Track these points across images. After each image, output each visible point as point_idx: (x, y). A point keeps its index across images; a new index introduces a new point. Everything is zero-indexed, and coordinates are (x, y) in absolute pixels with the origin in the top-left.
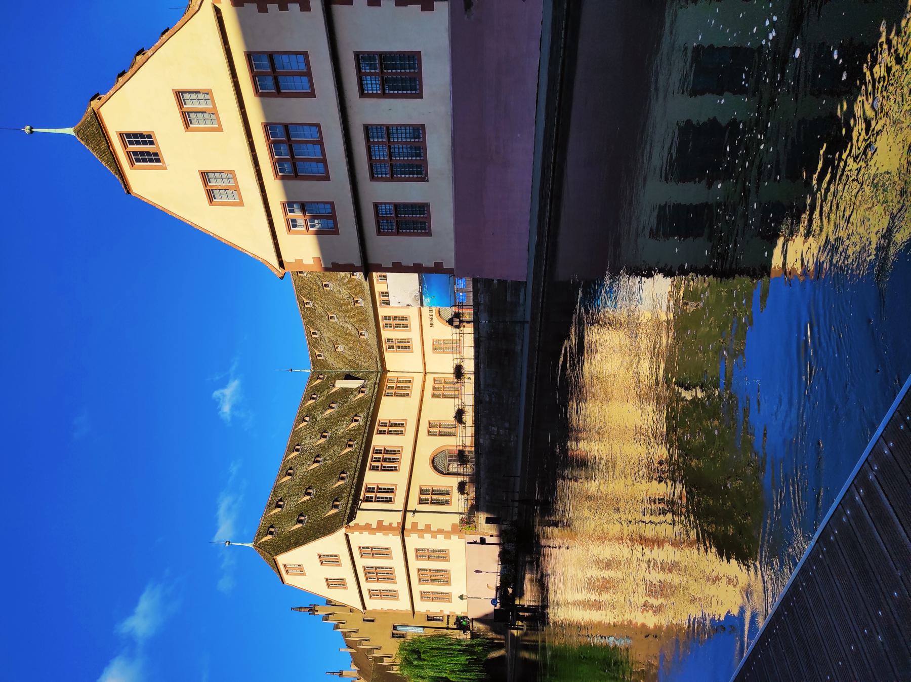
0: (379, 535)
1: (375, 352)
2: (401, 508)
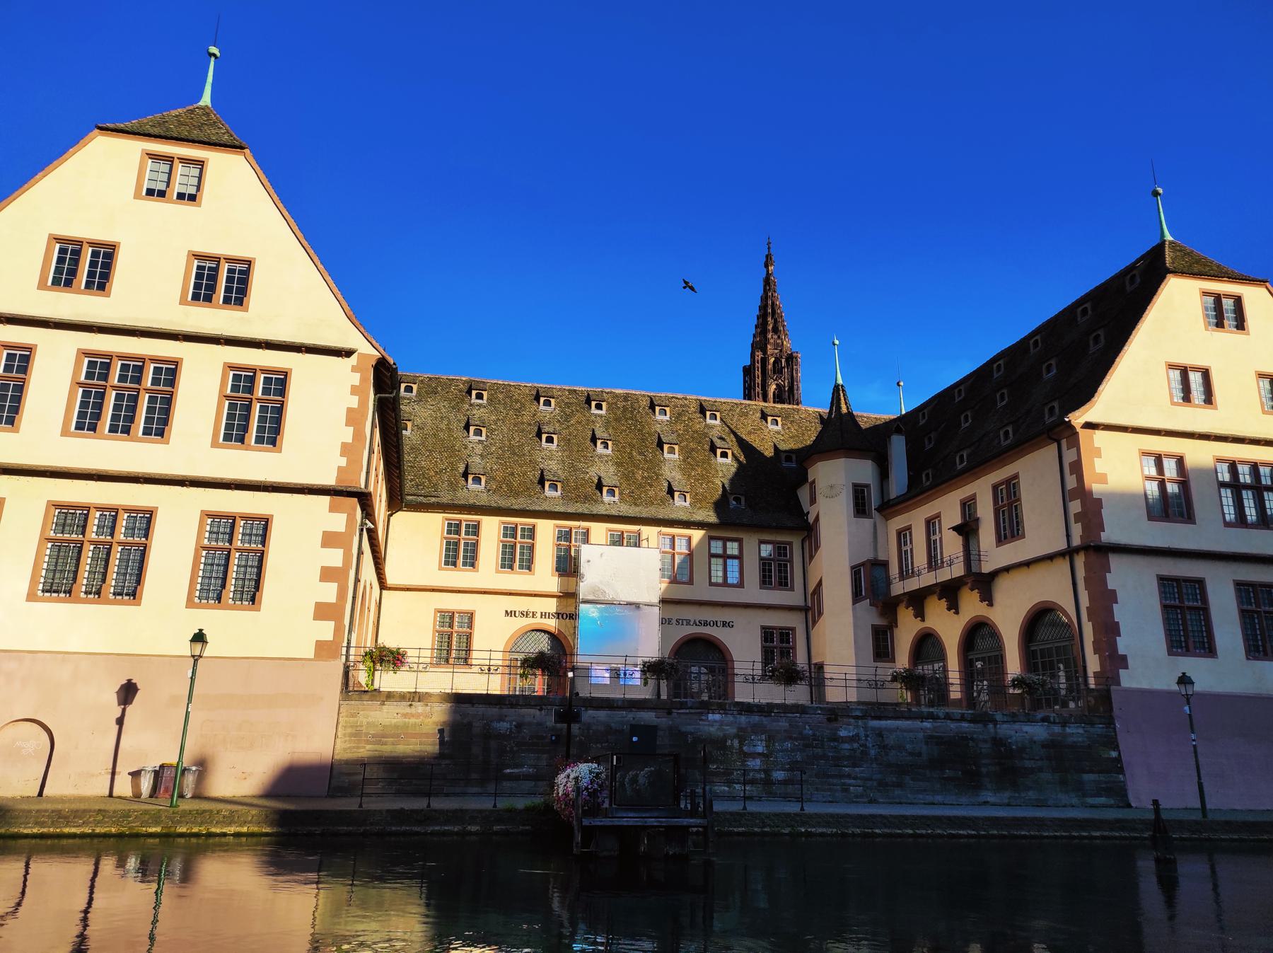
1: (445, 498)
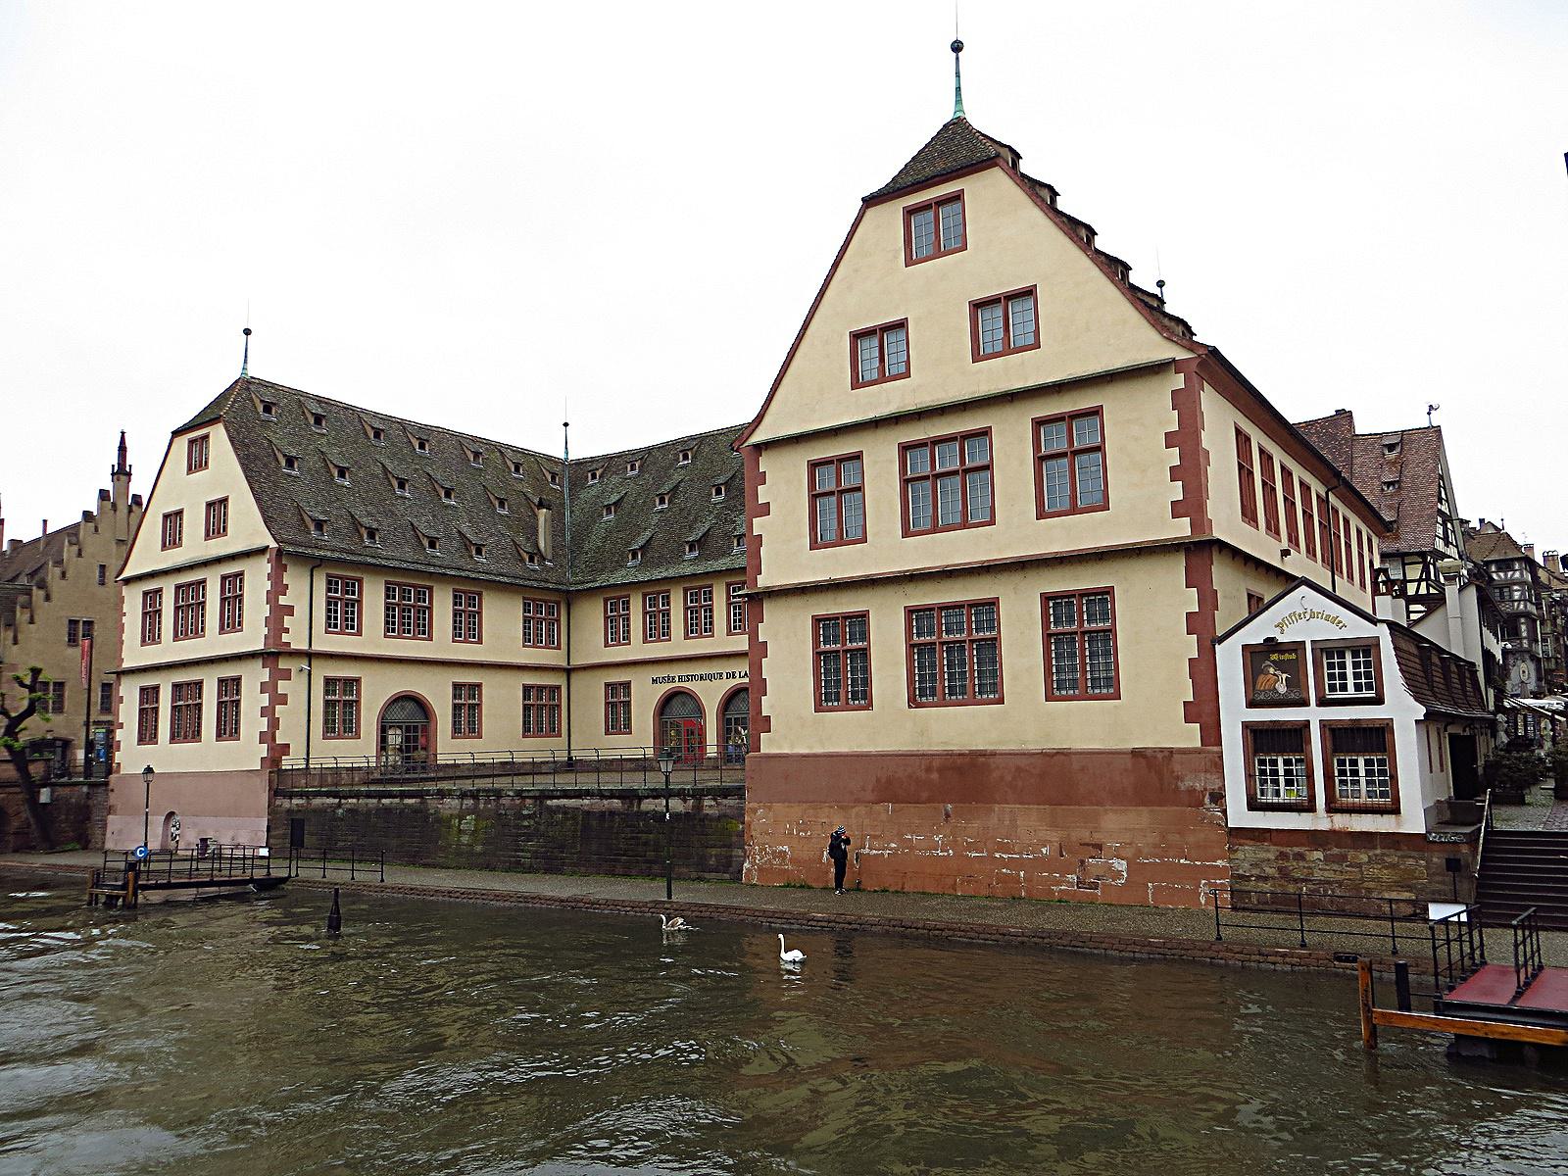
0: (266, 610)
2: (316, 647)
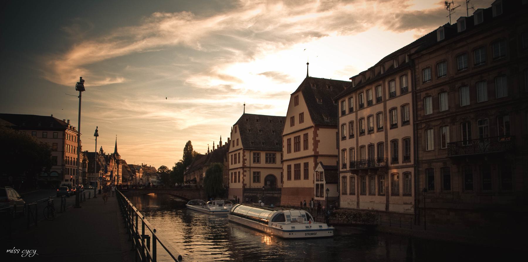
2: (251, 166)
